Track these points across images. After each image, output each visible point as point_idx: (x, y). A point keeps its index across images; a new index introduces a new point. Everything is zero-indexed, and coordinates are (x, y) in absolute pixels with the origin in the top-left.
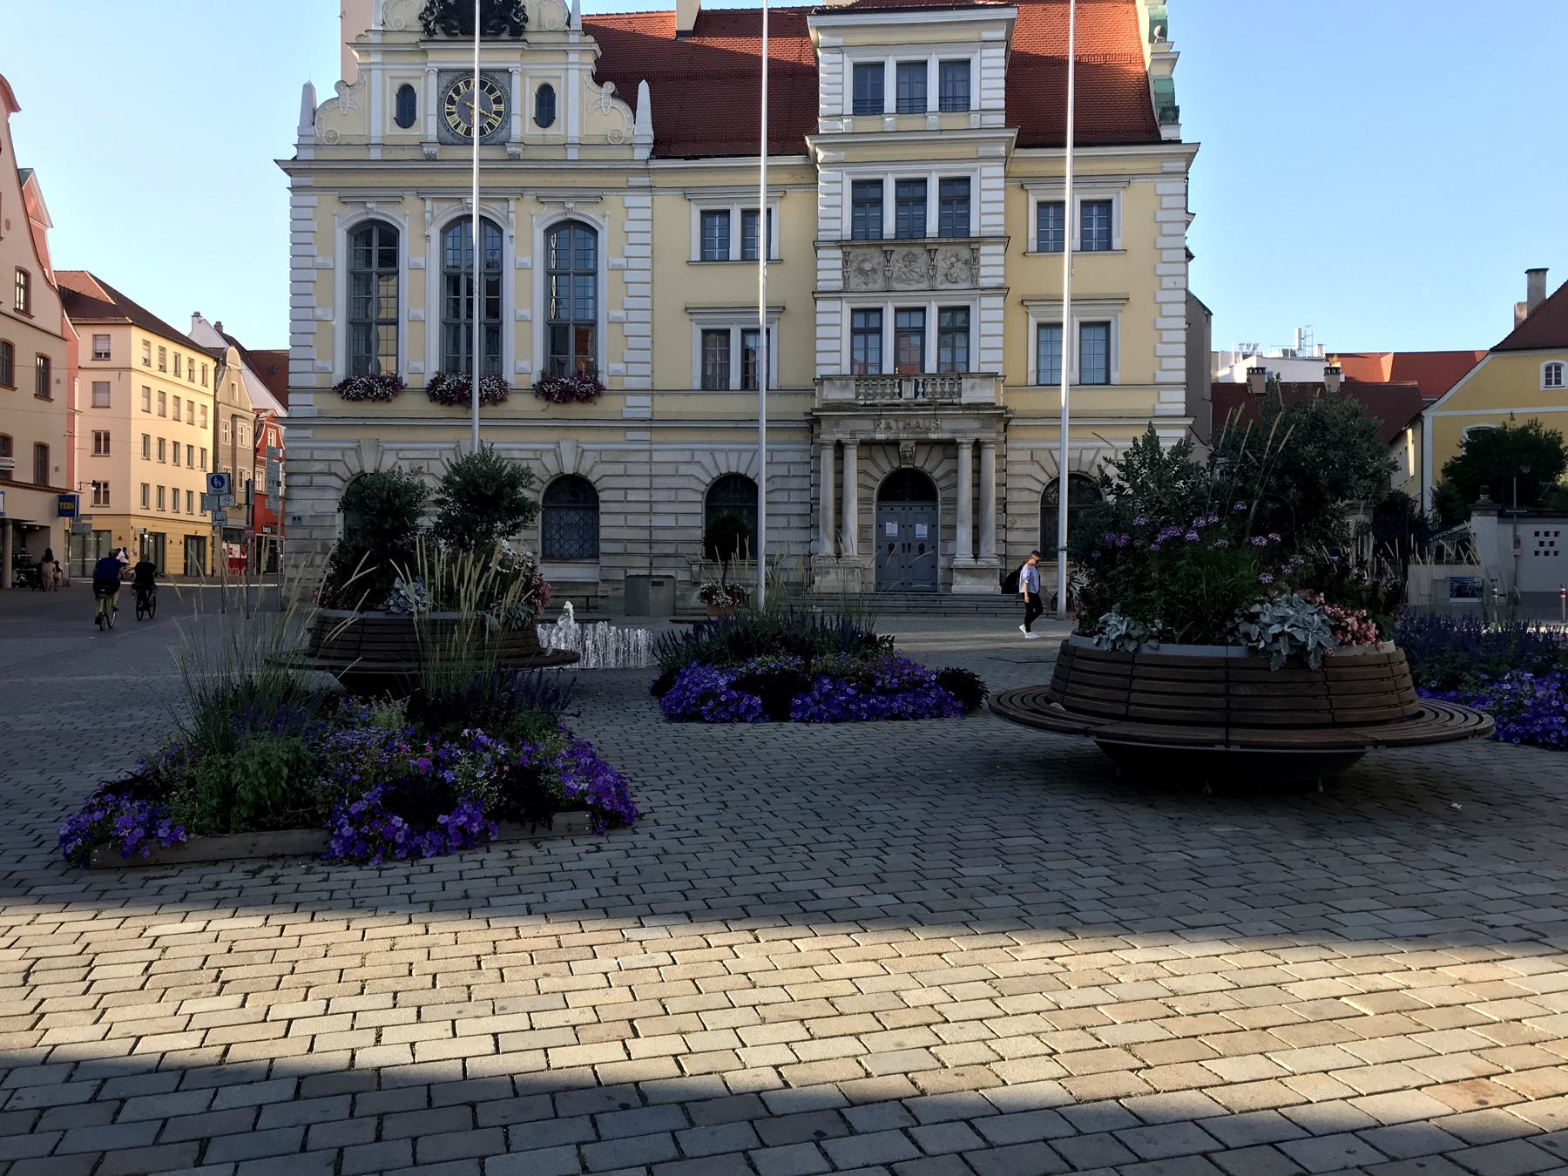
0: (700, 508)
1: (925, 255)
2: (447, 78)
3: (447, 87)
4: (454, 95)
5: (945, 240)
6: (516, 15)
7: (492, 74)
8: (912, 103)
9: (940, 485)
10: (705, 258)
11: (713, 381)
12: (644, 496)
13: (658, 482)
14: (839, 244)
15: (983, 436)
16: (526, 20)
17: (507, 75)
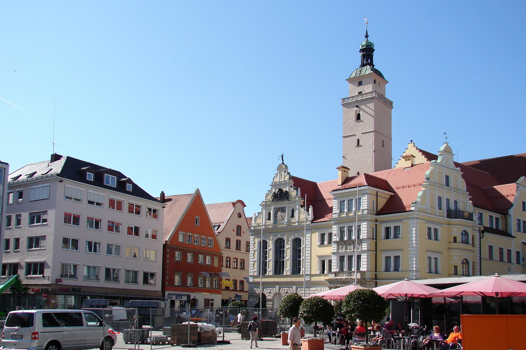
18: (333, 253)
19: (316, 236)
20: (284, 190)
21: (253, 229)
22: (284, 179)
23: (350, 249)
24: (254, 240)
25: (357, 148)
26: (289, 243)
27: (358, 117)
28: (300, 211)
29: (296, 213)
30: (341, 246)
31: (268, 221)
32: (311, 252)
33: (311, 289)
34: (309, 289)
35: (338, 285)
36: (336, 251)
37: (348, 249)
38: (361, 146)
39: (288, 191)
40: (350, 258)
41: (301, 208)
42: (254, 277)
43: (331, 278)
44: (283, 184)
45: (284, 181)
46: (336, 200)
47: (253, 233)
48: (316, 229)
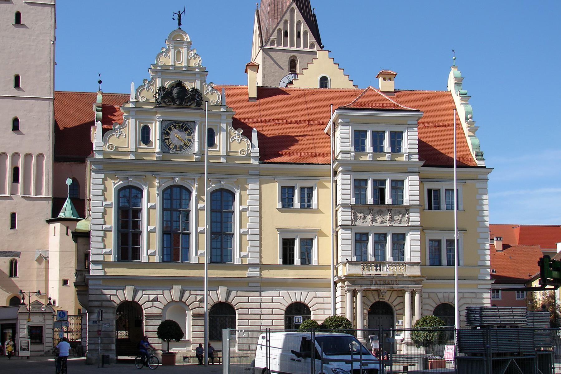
0: (283, 317)
1: (387, 211)
2: (165, 124)
3: (166, 127)
4: (169, 131)
6: (198, 97)
7: (186, 122)
8: (378, 147)
11: (288, 259)
12: (258, 311)
13: (263, 305)
15: (415, 289)
17: (193, 123)
20: (189, 86)
21: (101, 157)
22: (188, 61)
24: (103, 183)
26: (205, 198)
28: (231, 135)
29: (220, 139)
30: (362, 215)
31: (143, 146)
32: (260, 221)
33: (263, 294)
34: (259, 293)
35: (371, 286)
36: (349, 223)
37: (378, 220)
39: (199, 89)
41: (233, 130)
42: (105, 264)
43: (353, 273)
44: (184, 73)
45: (188, 67)
46: (348, 127)
47: (101, 167)
48: (274, 177)
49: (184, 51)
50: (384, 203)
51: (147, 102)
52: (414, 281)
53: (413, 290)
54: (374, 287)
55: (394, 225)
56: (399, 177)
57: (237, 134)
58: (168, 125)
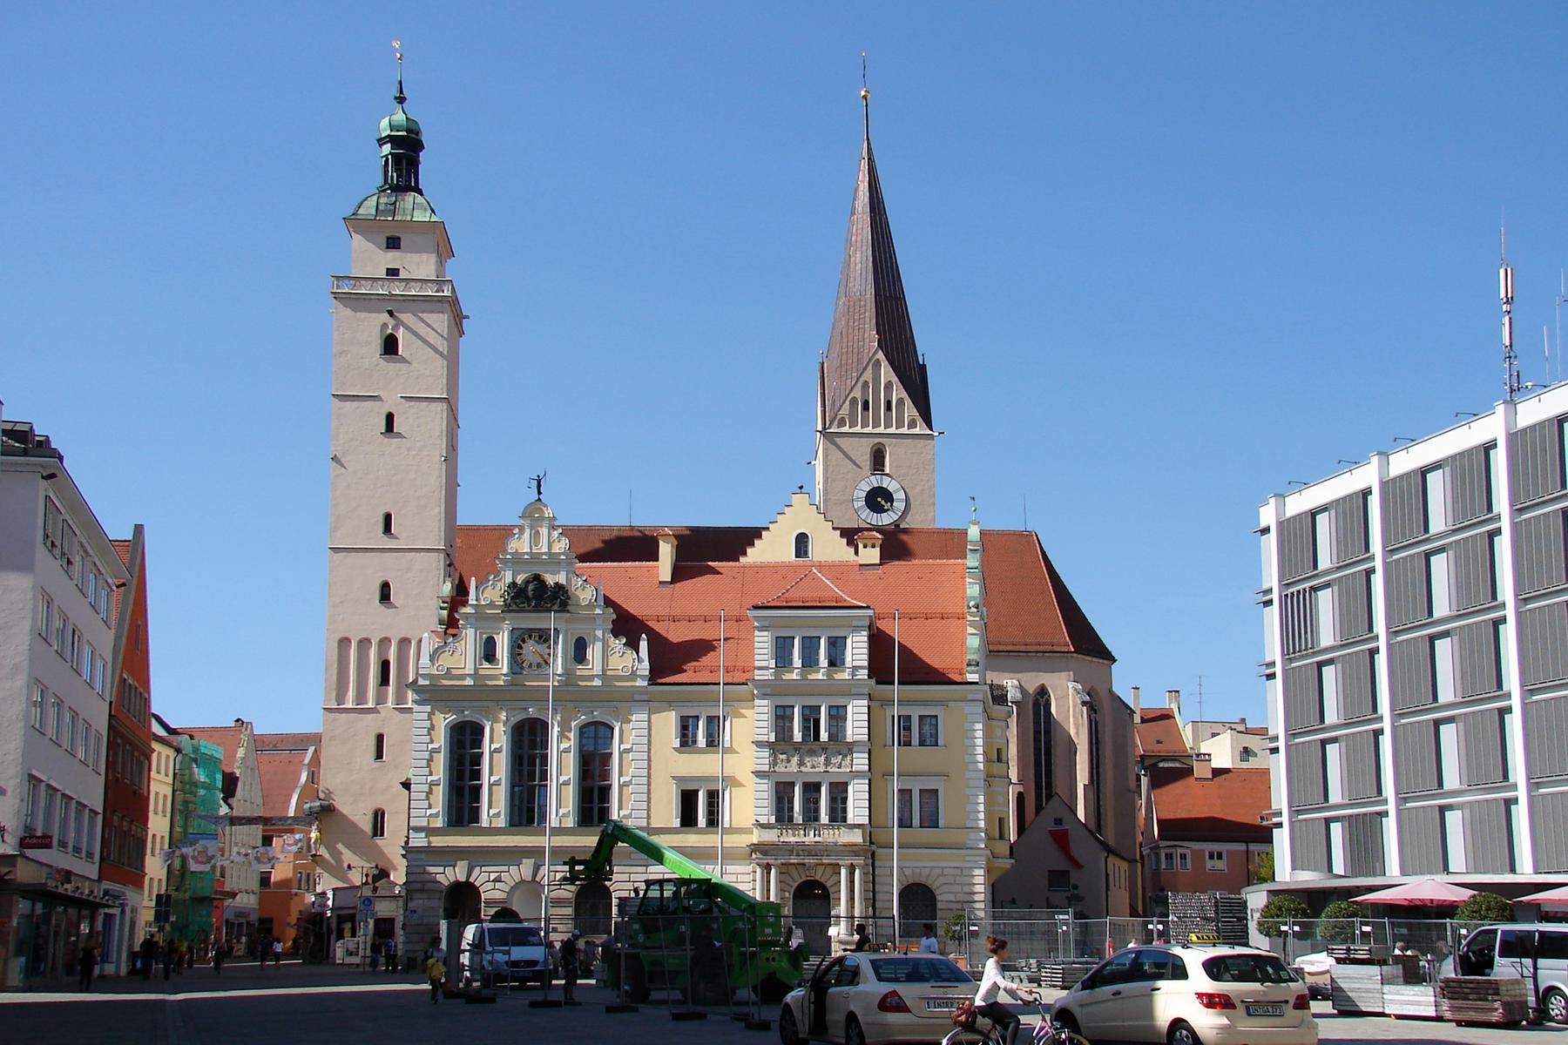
2: (516, 634)
5: (832, 743)
6: (563, 595)
8: (810, 661)
9: (831, 890)
10: (684, 743)
11: (688, 819)
14: (769, 745)
15: (854, 862)
16: (569, 599)
18: (757, 772)
19: (668, 723)
20: (551, 580)
21: (427, 683)
22: (550, 546)
23: (815, 766)
24: (430, 719)
25: (386, 440)
26: (572, 735)
27: (390, 346)
28: (609, 646)
29: (594, 653)
30: (784, 757)
31: (486, 665)
32: (649, 765)
34: (645, 868)
35: (790, 859)
36: (766, 768)
37: (808, 764)
38: (399, 435)
39: (565, 583)
40: (812, 789)
41: (613, 638)
42: (430, 831)
44: (544, 562)
45: (549, 553)
46: (766, 633)
47: (427, 696)
48: (670, 703)
49: (544, 531)
50: (819, 740)
51: (492, 605)
52: (853, 851)
53: (852, 864)
54: (794, 859)
55: (830, 770)
56: (840, 701)
57: (618, 644)
58: (520, 636)
